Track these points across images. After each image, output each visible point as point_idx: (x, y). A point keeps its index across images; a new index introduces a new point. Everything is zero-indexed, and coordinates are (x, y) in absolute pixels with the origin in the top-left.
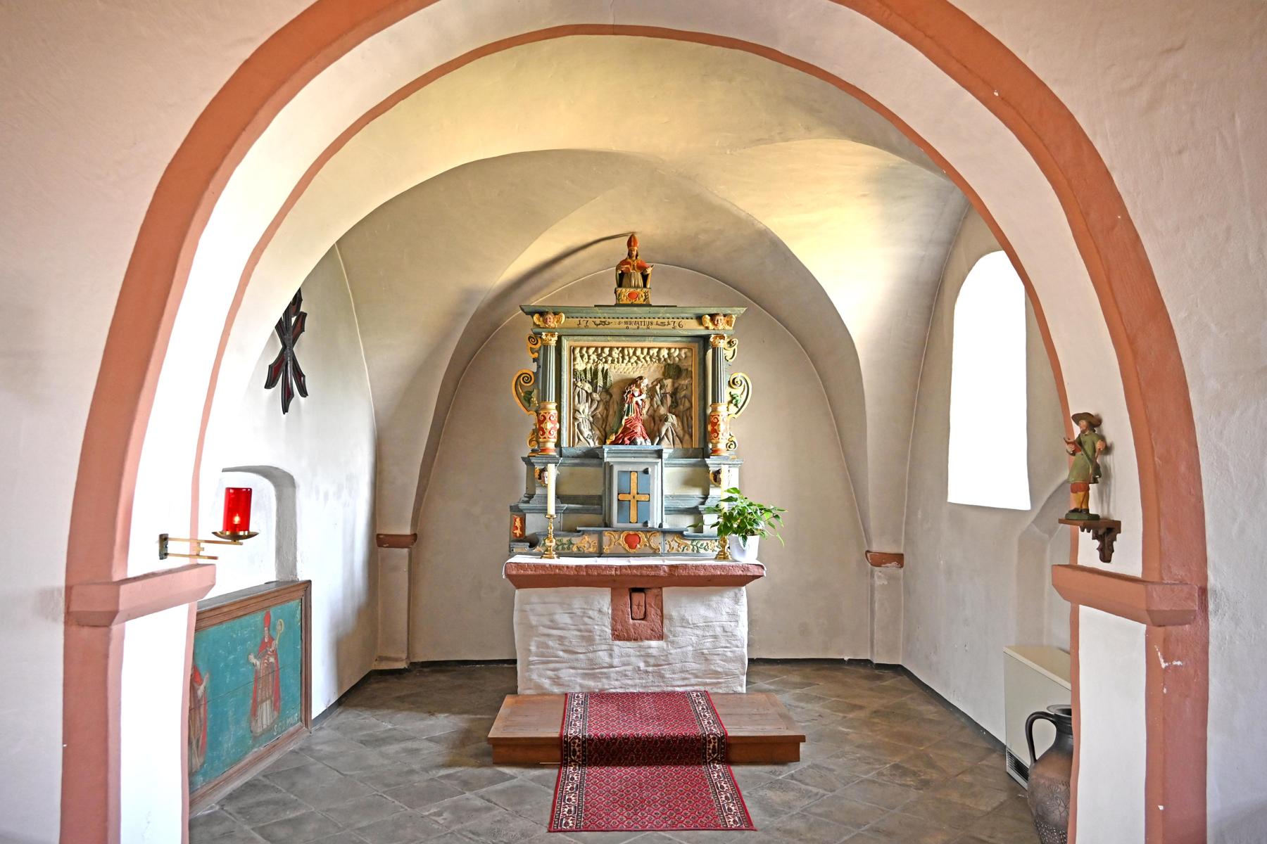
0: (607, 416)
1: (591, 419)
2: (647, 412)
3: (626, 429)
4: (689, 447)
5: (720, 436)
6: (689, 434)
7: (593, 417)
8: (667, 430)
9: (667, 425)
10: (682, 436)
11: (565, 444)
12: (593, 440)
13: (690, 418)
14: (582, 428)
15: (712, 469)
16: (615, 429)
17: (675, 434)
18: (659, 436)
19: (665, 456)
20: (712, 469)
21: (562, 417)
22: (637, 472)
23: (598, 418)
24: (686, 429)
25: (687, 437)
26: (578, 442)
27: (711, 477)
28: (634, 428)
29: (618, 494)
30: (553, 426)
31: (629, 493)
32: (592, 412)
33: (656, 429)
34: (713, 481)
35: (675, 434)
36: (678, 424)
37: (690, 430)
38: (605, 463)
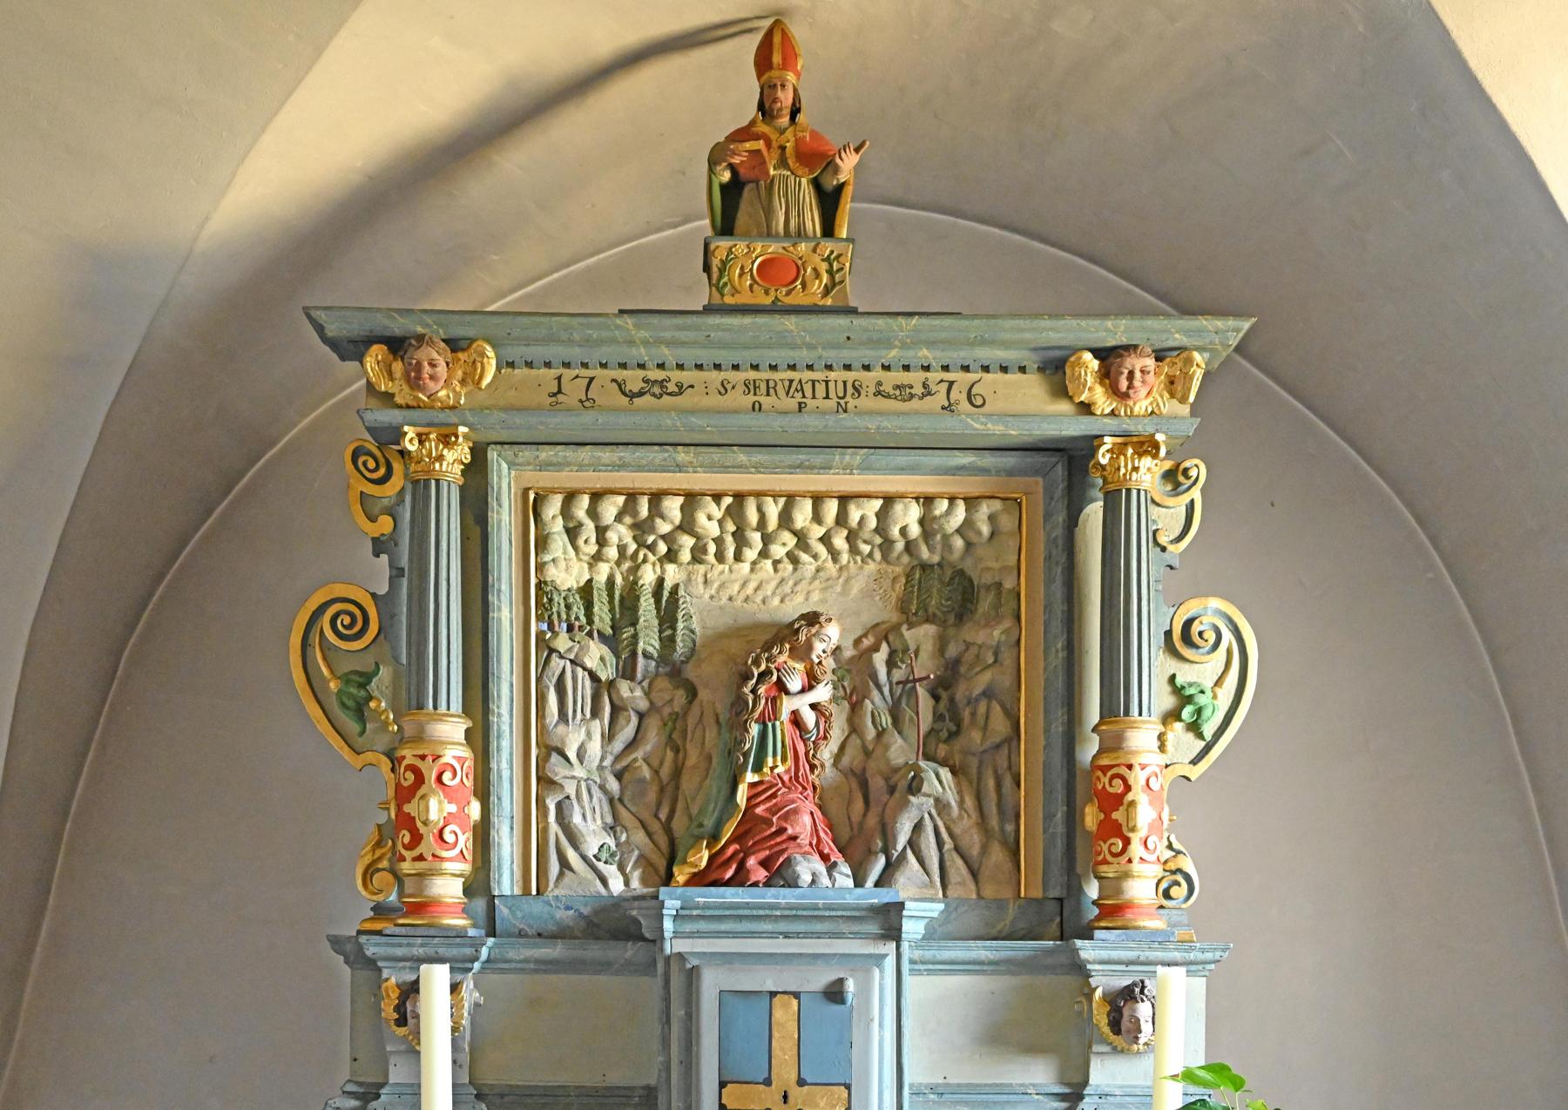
0: (677, 773)
1: (613, 785)
2: (837, 758)
3: (750, 822)
4: (1007, 893)
5: (1136, 849)
6: (1004, 843)
7: (619, 776)
8: (918, 827)
9: (920, 805)
10: (975, 852)
11: (506, 882)
12: (621, 868)
13: (1008, 782)
14: (577, 819)
15: (1103, 982)
16: (709, 823)
17: (949, 844)
18: (886, 851)
19: (912, 928)
20: (1103, 982)
21: (494, 777)
22: (796, 995)
23: (642, 781)
24: (994, 822)
25: (998, 855)
26: (561, 875)
27: (1101, 1018)
28: (786, 817)
29: (722, 1085)
30: (453, 808)
31: (768, 1082)
32: (618, 758)
33: (872, 821)
34: (1106, 1030)
35: (949, 844)
36: (961, 803)
37: (1010, 828)
38: (668, 959)
